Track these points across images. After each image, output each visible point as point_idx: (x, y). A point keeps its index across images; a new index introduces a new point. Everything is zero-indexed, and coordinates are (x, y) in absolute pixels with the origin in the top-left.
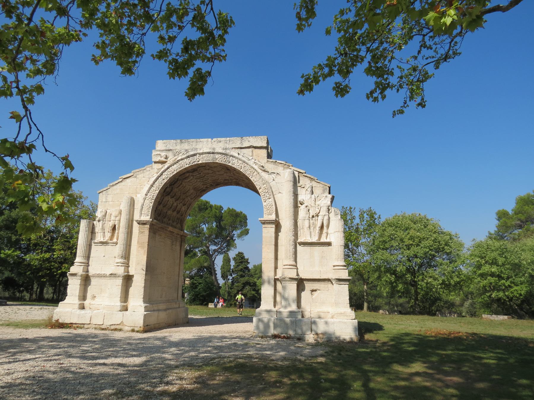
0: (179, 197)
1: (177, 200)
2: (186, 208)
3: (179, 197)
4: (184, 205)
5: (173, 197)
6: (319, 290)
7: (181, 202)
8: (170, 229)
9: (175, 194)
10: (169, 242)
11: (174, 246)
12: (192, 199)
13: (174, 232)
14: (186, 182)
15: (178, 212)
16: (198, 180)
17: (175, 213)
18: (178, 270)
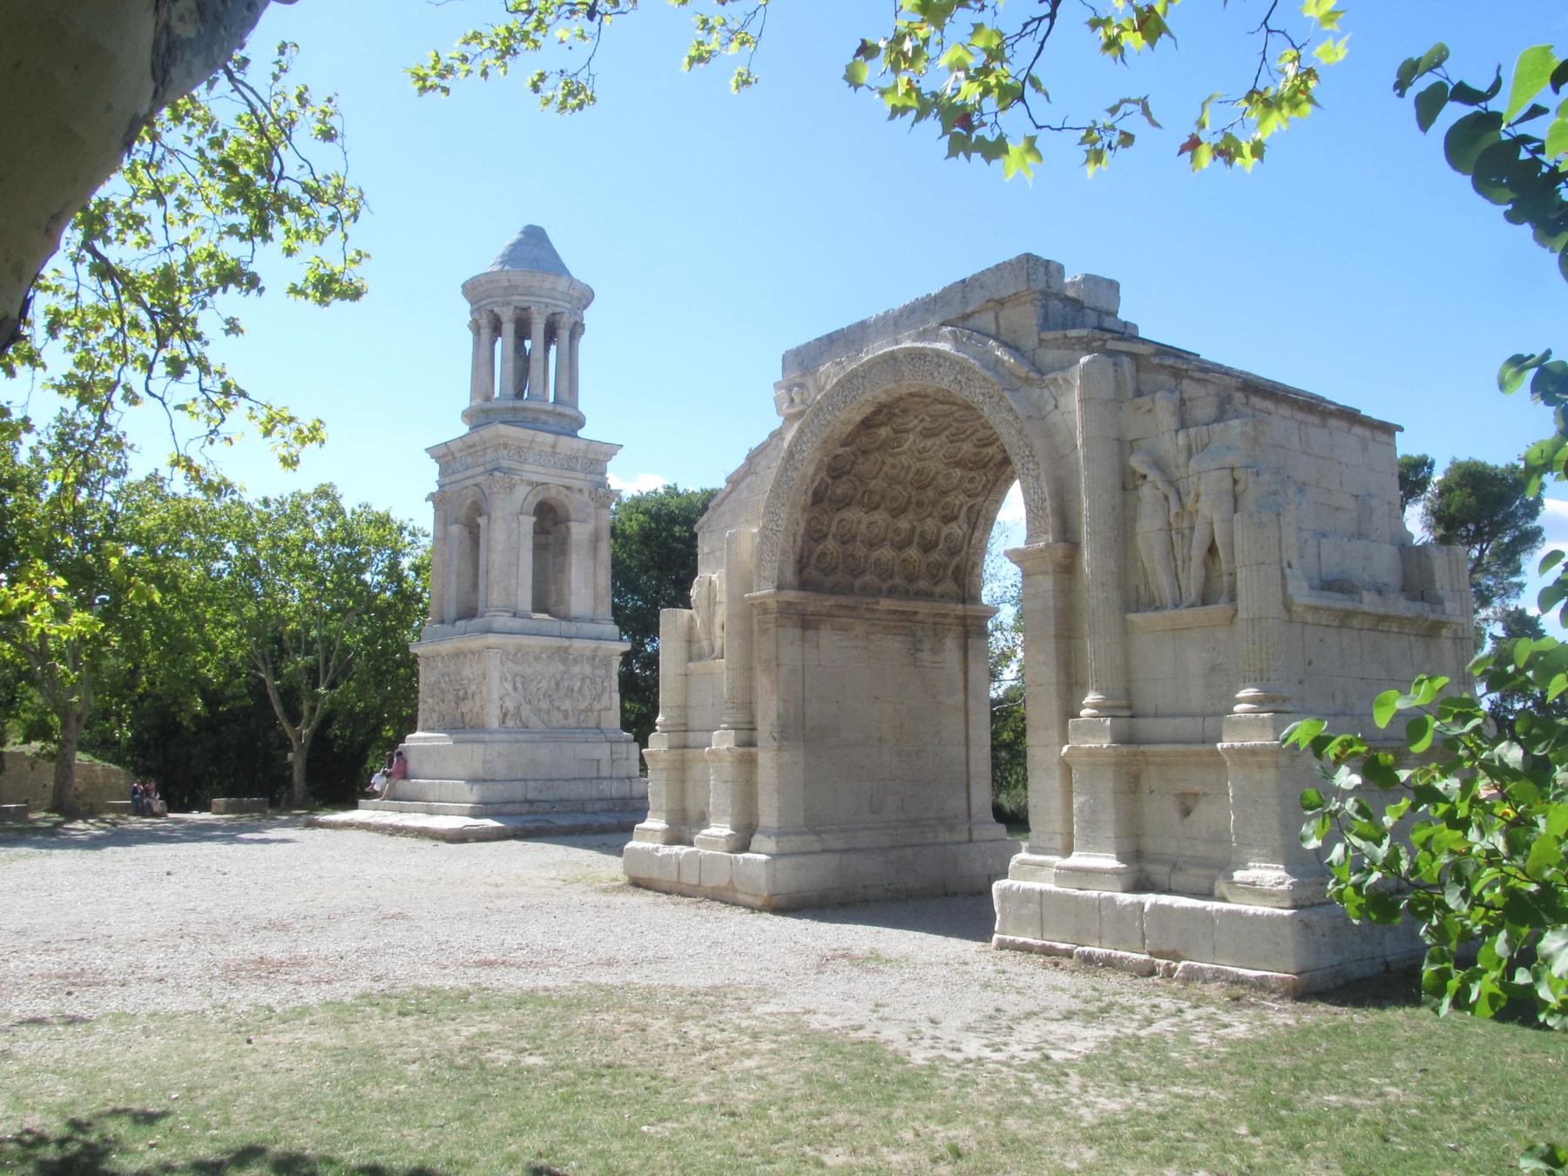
0: (909, 503)
1: (904, 511)
2: (965, 527)
3: (909, 503)
4: (949, 519)
5: (877, 507)
6: (1205, 794)
7: (930, 515)
8: (885, 604)
9: (883, 497)
10: (894, 645)
11: (926, 656)
12: (977, 495)
13: (916, 613)
14: (899, 454)
15: (927, 547)
16: (943, 438)
17: (913, 552)
18: (962, 725)
